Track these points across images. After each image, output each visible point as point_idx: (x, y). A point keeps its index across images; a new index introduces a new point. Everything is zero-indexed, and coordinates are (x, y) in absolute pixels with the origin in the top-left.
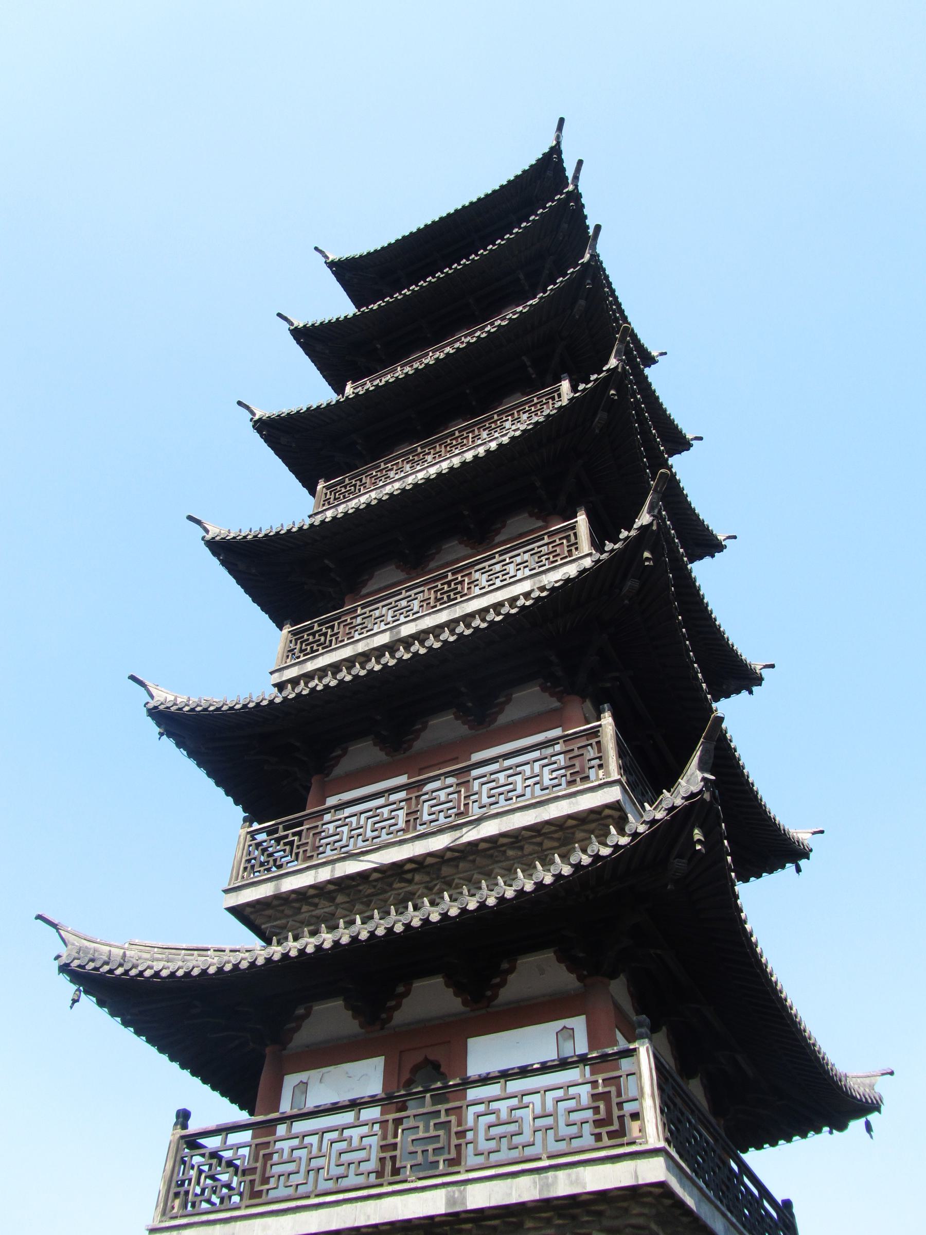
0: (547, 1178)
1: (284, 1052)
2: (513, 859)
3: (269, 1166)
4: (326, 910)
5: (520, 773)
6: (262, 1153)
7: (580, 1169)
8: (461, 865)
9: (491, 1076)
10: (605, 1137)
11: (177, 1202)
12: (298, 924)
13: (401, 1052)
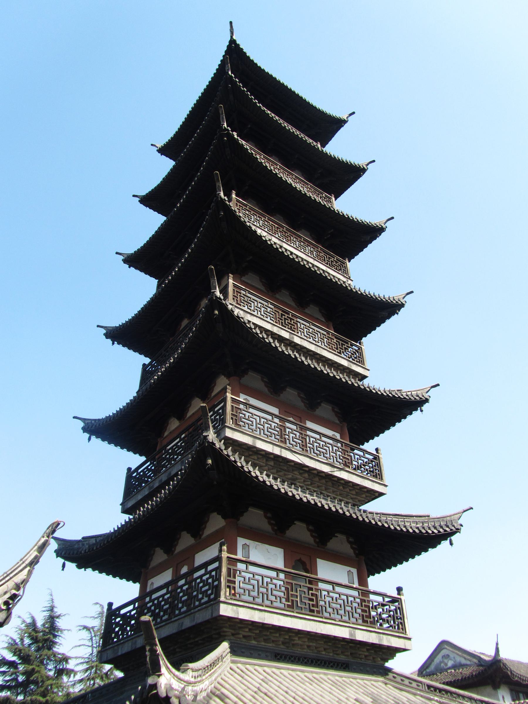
7: (390, 637)
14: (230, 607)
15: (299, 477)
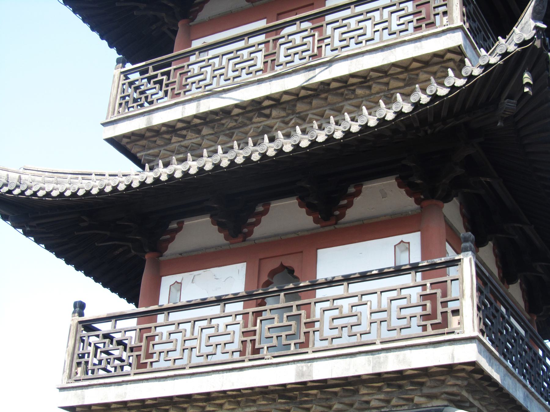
0: (379, 358)
1: (160, 258)
2: (362, 97)
3: (151, 345)
4: (193, 141)
5: (210, 65)
6: (145, 335)
7: (407, 352)
8: (315, 102)
9: (336, 279)
10: (429, 328)
11: (80, 370)
12: (169, 153)
13: (260, 259)
14: (72, 392)
15: (269, 122)
